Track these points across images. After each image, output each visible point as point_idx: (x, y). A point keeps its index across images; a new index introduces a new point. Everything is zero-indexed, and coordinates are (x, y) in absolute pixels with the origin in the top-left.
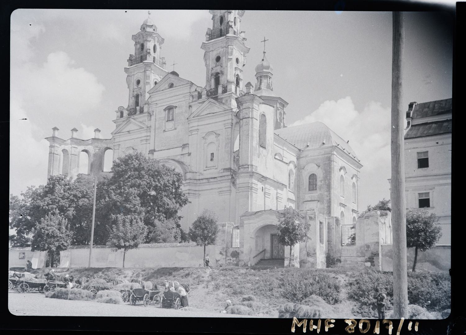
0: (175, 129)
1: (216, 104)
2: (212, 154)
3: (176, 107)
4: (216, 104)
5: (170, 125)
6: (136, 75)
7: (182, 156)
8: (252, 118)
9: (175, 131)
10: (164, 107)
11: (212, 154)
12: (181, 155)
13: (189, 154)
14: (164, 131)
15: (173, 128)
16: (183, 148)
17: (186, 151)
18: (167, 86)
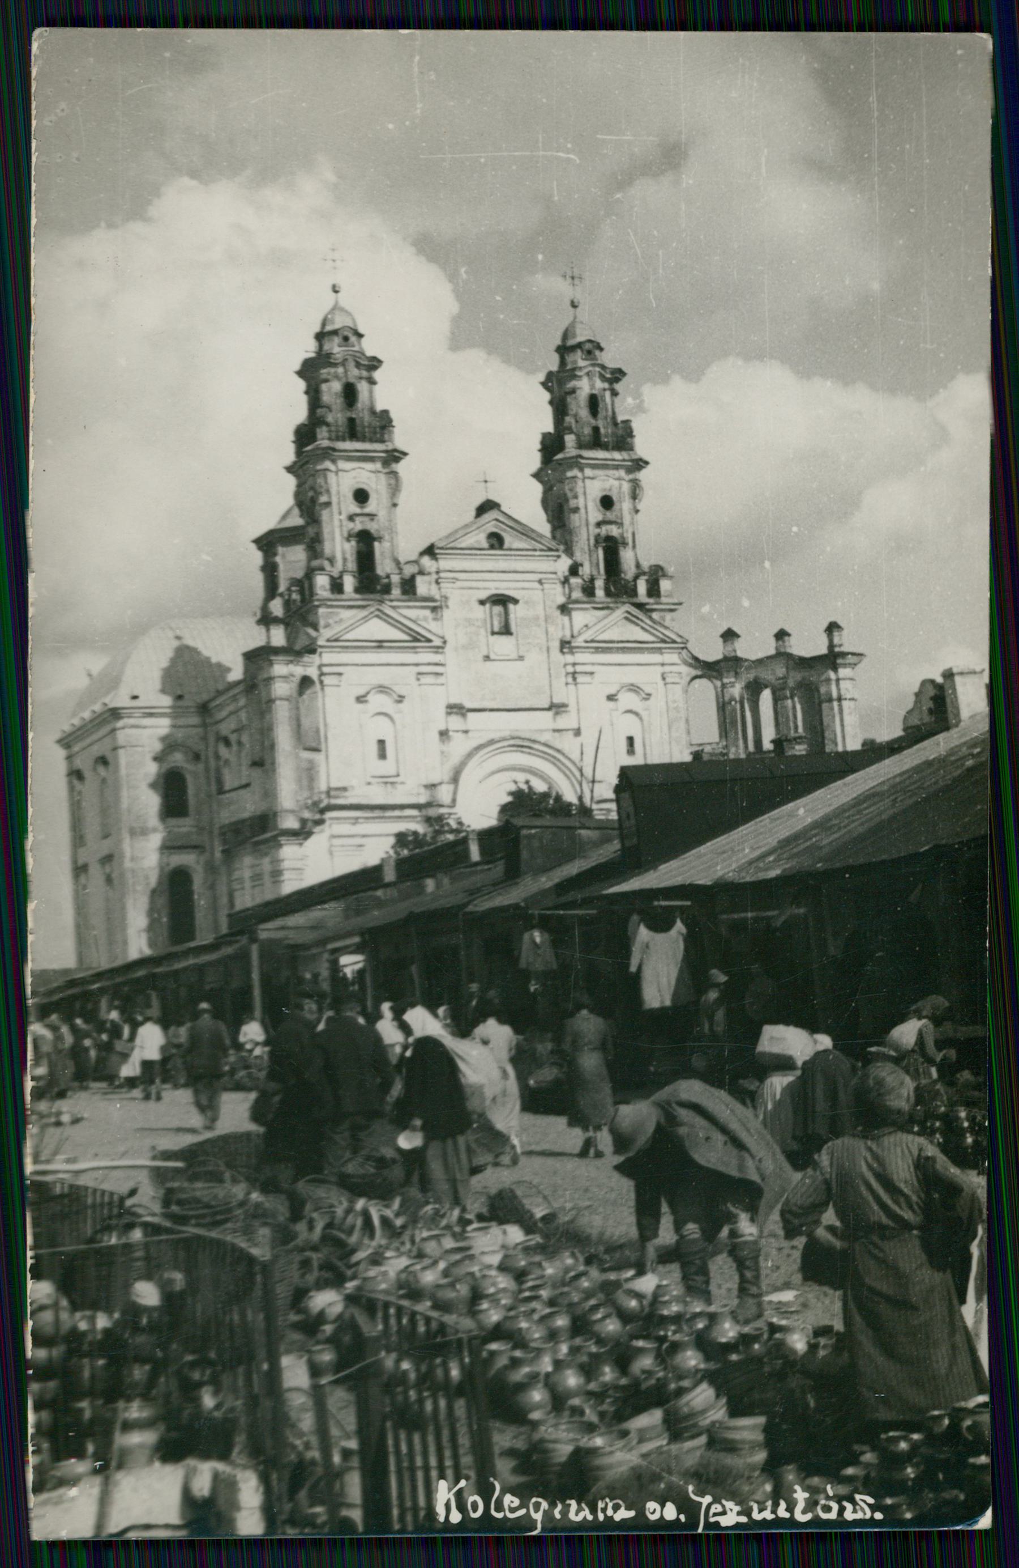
0: (521, 658)
1: (642, 621)
2: (631, 740)
3: (516, 601)
4: (642, 621)
5: (503, 645)
6: (353, 473)
7: (557, 734)
8: (840, 699)
9: (519, 663)
10: (484, 595)
11: (631, 740)
12: (555, 731)
13: (578, 732)
14: (487, 658)
15: (514, 656)
16: (557, 713)
17: (563, 722)
18: (480, 538)
